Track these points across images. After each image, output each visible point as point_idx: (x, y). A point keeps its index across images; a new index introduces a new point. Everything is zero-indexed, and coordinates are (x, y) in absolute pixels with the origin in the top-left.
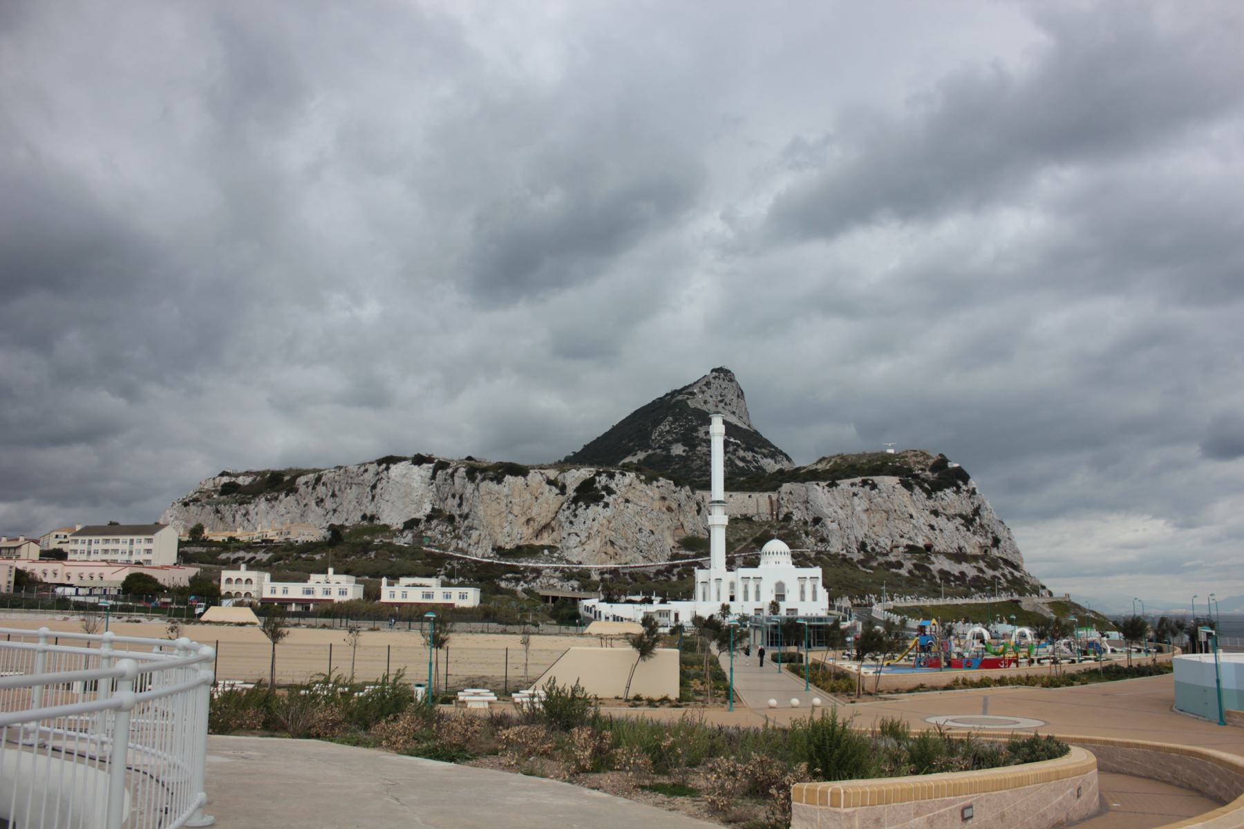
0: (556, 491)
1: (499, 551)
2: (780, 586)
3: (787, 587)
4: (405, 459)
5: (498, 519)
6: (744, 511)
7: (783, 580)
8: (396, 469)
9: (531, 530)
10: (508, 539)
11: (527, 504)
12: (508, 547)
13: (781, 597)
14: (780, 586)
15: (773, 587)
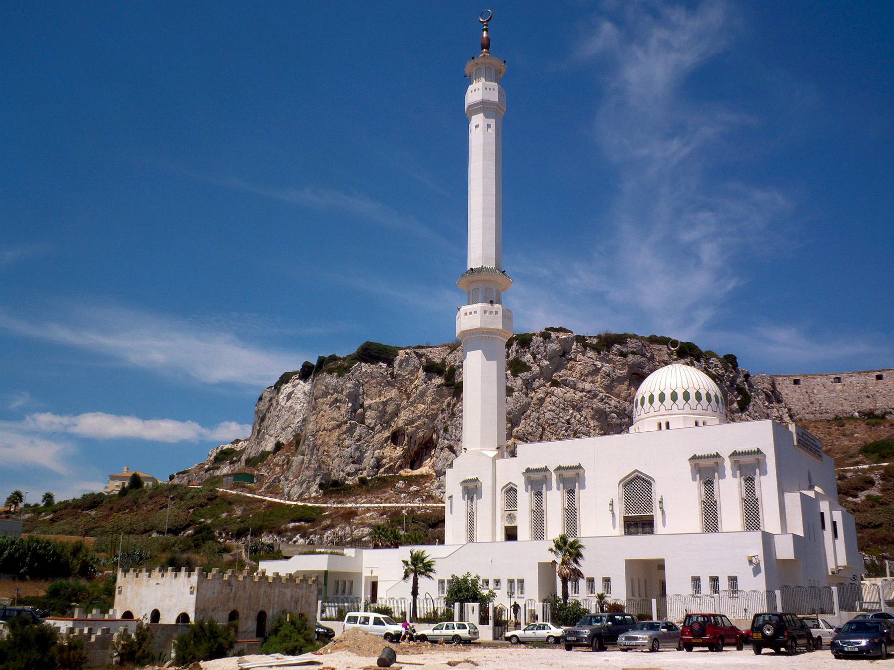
0: (439, 381)
1: (333, 488)
2: (637, 486)
3: (658, 491)
4: (294, 373)
5: (337, 432)
6: (867, 405)
7: (646, 471)
8: (287, 388)
9: (399, 451)
10: (351, 468)
11: (390, 409)
12: (350, 482)
13: (639, 524)
14: (637, 486)
15: (616, 493)
